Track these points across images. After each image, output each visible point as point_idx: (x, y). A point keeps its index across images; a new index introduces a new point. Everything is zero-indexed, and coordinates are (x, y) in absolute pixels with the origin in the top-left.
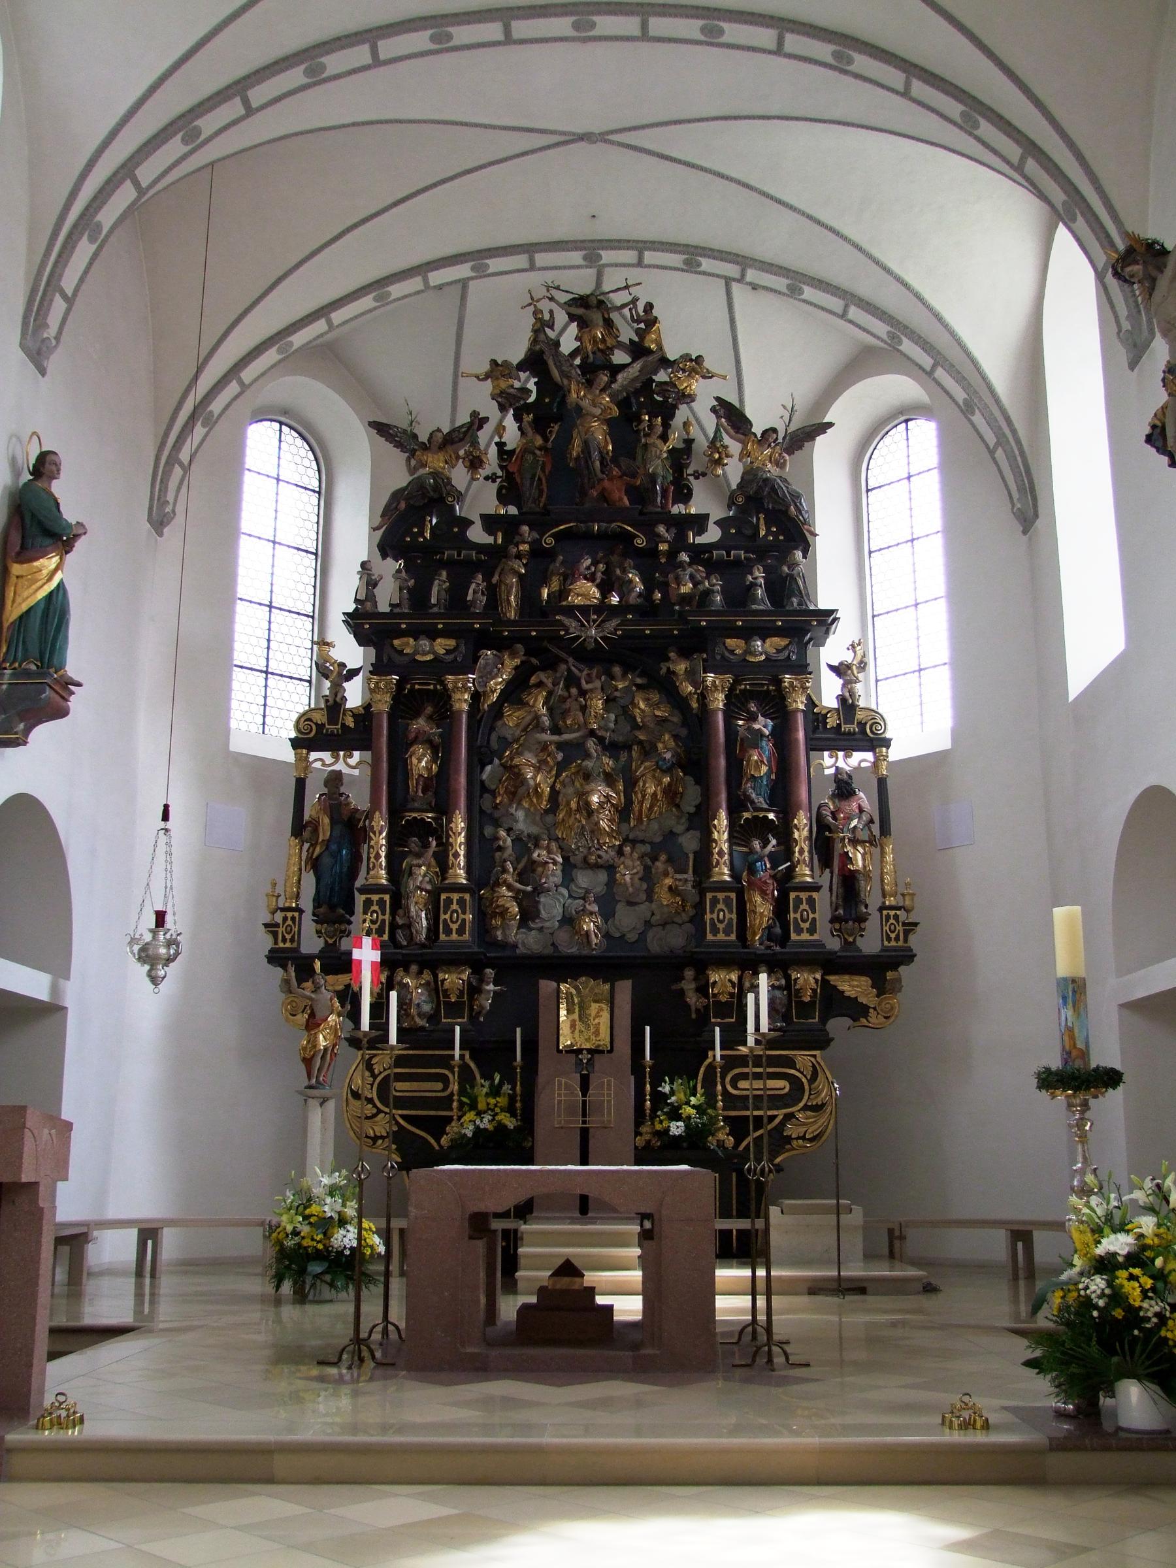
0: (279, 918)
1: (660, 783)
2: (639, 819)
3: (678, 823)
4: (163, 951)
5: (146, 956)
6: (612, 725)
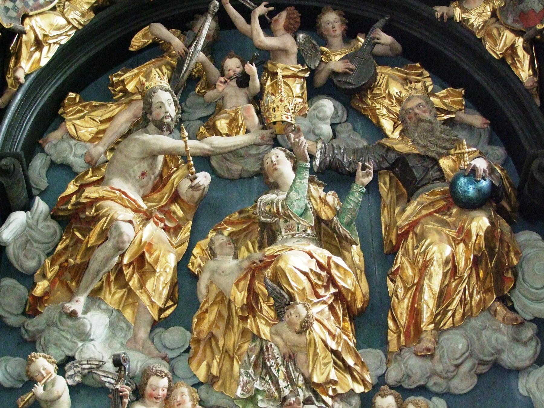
1: (464, 236)
2: (414, 330)
3: (516, 340)
6: (326, 129)
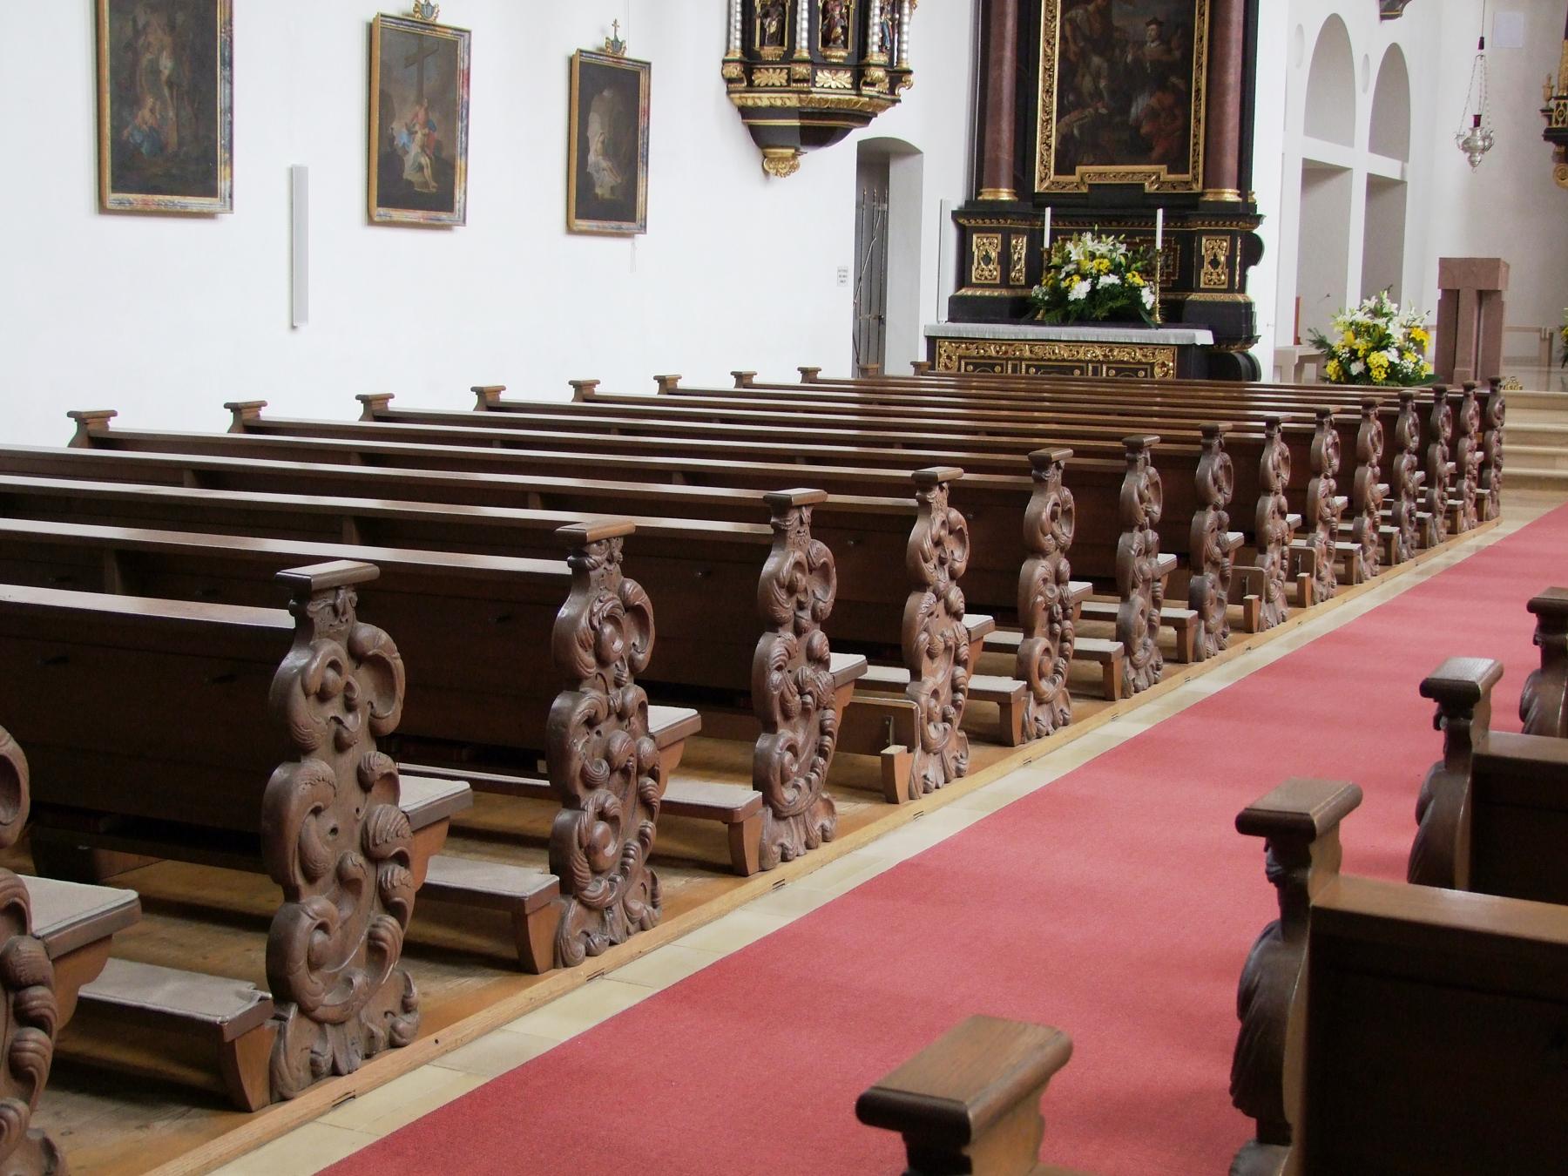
0: (1553, 104)
4: (1480, 143)
5: (1467, 147)
